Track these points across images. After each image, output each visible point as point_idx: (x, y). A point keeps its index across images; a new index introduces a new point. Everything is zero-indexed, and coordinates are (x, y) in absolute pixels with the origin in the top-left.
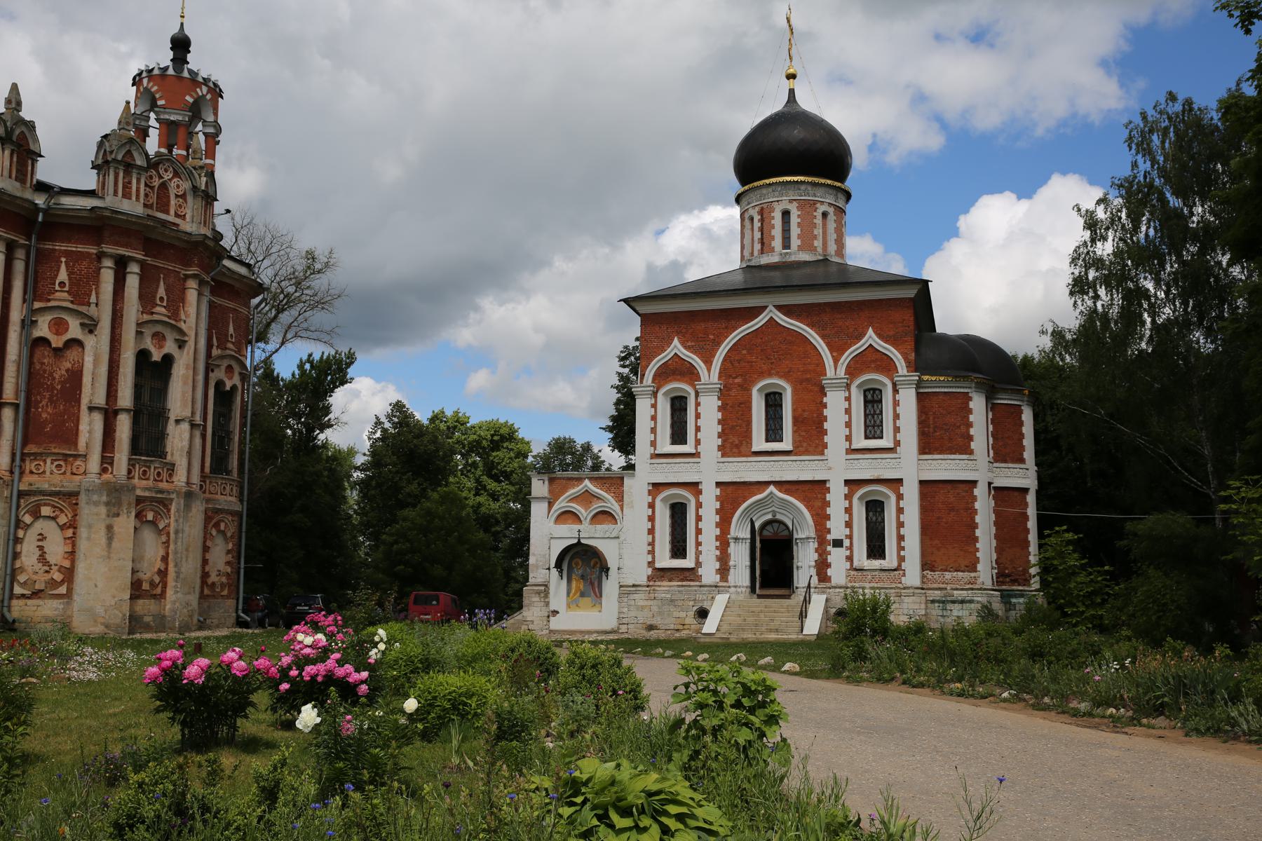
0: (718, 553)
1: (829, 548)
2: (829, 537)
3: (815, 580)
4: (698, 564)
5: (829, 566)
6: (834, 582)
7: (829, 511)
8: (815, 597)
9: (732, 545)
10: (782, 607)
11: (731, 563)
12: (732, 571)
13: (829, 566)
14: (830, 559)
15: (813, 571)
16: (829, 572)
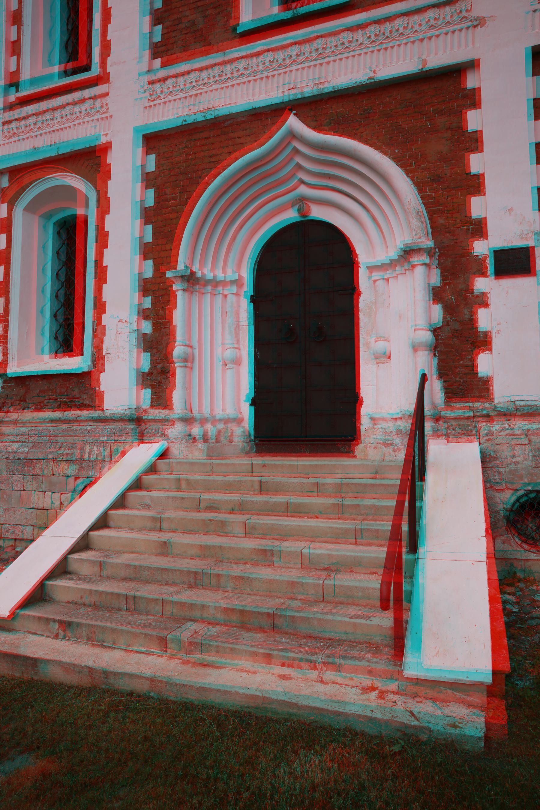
0: (147, 327)
1: (481, 285)
2: (481, 248)
3: (436, 390)
4: (98, 359)
5: (484, 342)
6: (502, 393)
7: (476, 163)
8: (436, 449)
9: (181, 298)
10: (318, 490)
11: (178, 351)
12: (179, 373)
13: (484, 342)
14: (484, 320)
15: (425, 362)
16: (485, 364)
